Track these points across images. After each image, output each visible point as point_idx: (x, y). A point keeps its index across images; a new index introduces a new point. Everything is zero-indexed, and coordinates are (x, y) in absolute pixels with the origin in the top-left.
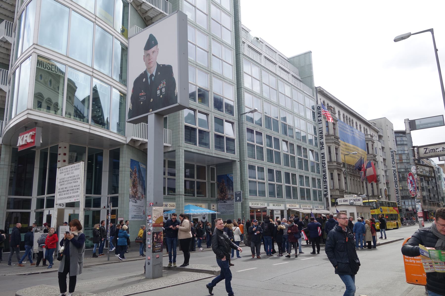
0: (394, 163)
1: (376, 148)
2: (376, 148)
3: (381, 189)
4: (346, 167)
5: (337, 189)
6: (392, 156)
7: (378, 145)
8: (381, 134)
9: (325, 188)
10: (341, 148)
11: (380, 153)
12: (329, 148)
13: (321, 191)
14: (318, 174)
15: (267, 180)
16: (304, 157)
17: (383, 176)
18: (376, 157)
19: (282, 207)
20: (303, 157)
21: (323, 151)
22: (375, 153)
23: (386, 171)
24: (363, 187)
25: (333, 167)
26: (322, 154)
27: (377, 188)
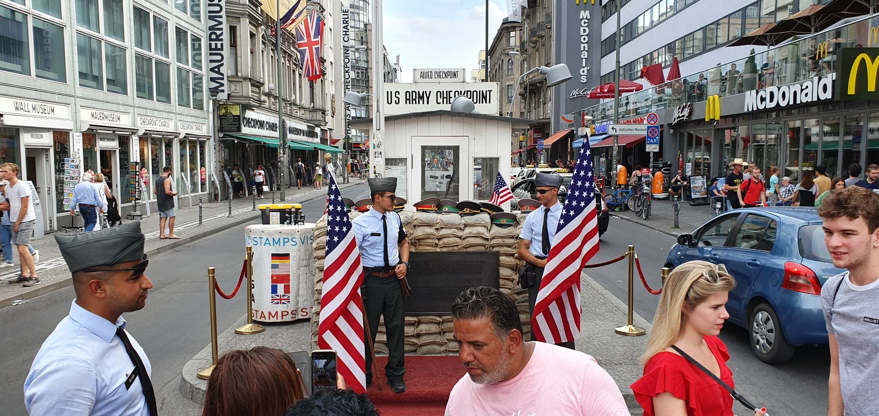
0: (346, 39)
5: (245, 79)
6: (346, 22)
9: (212, 70)
13: (201, 79)
14: (194, 21)
19: (60, 117)
25: (239, 9)
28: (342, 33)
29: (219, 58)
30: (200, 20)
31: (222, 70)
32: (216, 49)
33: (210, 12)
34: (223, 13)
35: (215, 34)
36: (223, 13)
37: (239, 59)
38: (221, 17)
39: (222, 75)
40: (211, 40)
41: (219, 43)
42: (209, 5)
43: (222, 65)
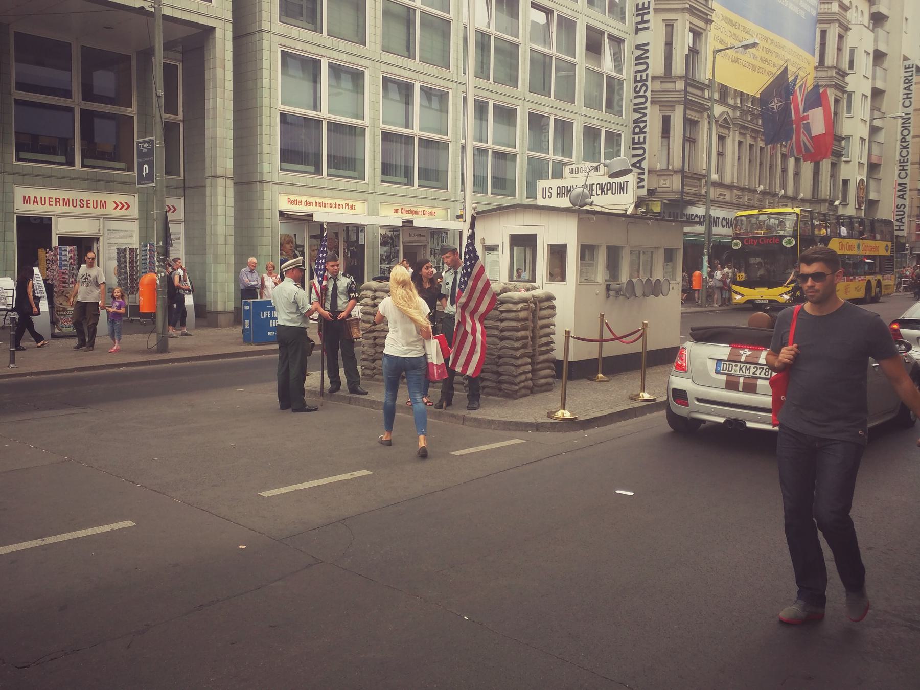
1: (852, 52)
2: (852, 52)
3: (846, 182)
4: (731, 101)
5: (676, 172)
6: (908, 81)
7: (862, 39)
8: (884, 10)
10: (718, 33)
11: (864, 63)
12: (670, 26)
15: (374, 119)
16: (559, 49)
17: (863, 140)
18: (848, 79)
20: (553, 51)
21: (643, 37)
22: (845, 65)
23: (874, 130)
24: (784, 171)
26: (638, 47)
27: (833, 176)
28: (901, 96)
29: (641, 152)
30: (621, 116)
31: (645, 165)
32: (639, 143)
33: (635, 104)
34: (648, 104)
35: (639, 127)
36: (648, 104)
37: (671, 150)
38: (646, 108)
39: (644, 169)
40: (634, 133)
41: (642, 136)
42: (635, 97)
43: (644, 159)
